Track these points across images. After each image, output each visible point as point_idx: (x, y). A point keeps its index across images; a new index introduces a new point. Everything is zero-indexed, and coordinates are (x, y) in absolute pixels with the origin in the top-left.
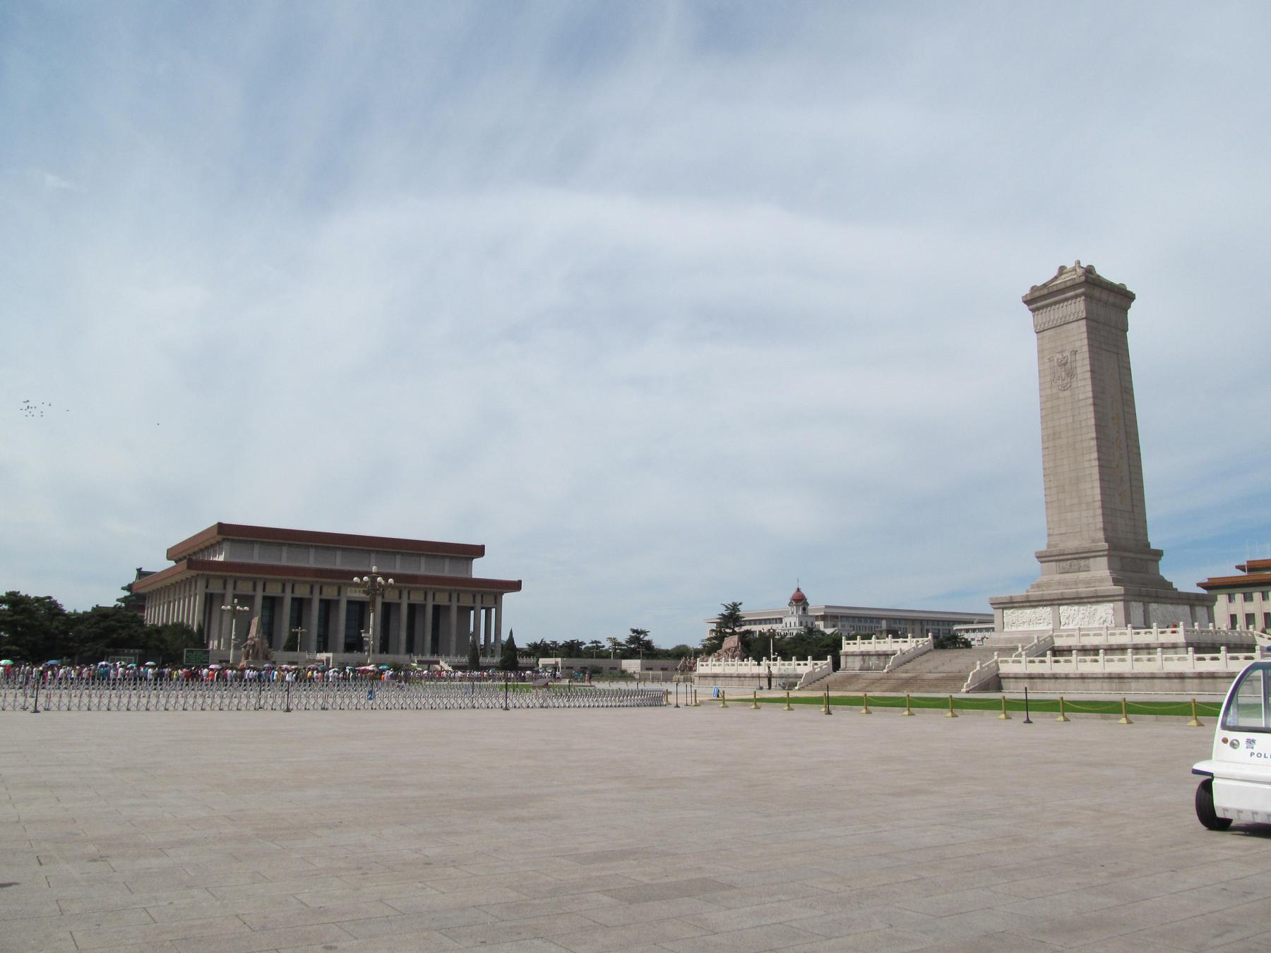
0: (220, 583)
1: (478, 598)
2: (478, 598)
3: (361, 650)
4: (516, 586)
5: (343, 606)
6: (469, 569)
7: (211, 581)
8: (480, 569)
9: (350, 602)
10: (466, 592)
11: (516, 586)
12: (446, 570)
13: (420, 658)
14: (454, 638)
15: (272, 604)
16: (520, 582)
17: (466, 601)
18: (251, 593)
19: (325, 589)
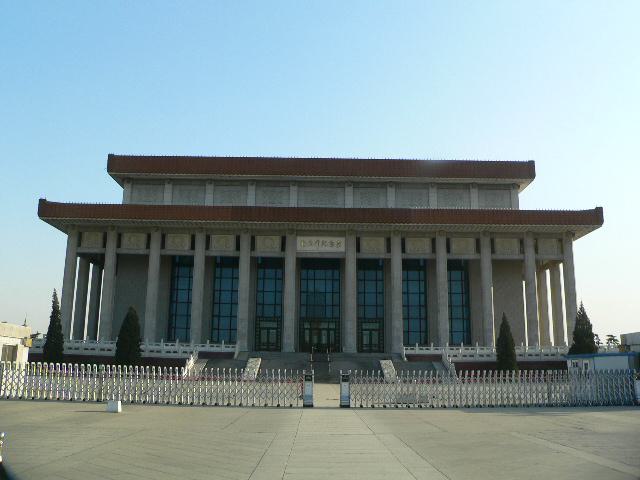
1: (529, 242)
2: (529, 242)
4: (592, 219)
5: (290, 267)
7: (86, 235)
8: (530, 199)
9: (306, 263)
10: (505, 235)
11: (592, 219)
12: (475, 202)
13: (417, 350)
15: (178, 266)
17: (508, 249)
18: (142, 252)
19: (259, 240)
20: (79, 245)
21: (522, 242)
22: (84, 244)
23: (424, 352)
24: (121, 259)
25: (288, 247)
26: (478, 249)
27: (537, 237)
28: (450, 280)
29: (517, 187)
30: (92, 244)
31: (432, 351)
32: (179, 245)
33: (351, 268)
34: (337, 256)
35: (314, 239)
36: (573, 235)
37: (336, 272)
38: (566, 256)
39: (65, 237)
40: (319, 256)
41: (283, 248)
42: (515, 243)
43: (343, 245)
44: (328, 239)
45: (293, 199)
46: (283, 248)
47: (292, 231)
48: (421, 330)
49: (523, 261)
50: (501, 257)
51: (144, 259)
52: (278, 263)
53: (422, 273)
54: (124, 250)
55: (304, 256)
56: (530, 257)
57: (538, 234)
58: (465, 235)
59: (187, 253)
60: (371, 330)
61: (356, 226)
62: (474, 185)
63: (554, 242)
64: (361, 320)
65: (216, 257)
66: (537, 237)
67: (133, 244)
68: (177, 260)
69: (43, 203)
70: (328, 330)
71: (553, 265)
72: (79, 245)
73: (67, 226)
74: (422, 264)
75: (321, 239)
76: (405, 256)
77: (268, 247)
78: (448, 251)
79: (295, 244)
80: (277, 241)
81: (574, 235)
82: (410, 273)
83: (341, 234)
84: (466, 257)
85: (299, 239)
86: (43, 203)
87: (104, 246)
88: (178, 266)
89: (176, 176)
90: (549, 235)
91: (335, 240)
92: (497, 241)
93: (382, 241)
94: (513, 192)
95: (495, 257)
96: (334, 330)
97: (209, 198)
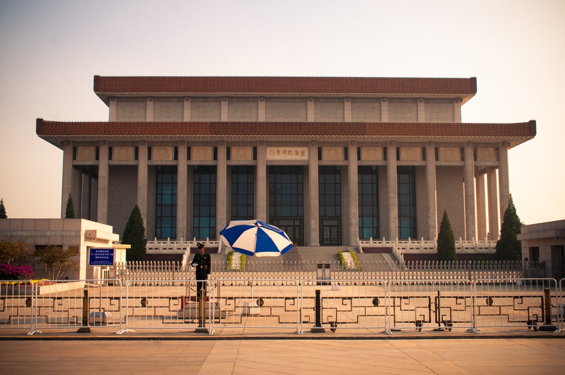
0: (92, 151)
1: (469, 152)
2: (469, 152)
3: (400, 238)
4: (527, 130)
6: (456, 113)
8: (471, 112)
9: (273, 170)
11: (527, 130)
12: (423, 115)
14: (394, 213)
15: (163, 175)
16: (532, 124)
17: (450, 157)
18: (132, 163)
20: (74, 158)
21: (462, 150)
22: (79, 156)
23: (378, 245)
24: (114, 170)
25: (259, 156)
26: (424, 157)
27: (476, 146)
28: (399, 183)
29: (460, 101)
30: (86, 157)
31: (384, 244)
32: (163, 157)
33: (314, 174)
34: (301, 164)
35: (281, 149)
36: (509, 145)
37: (300, 176)
38: (501, 163)
39: (62, 151)
41: (255, 157)
42: (457, 151)
43: (306, 154)
44: (293, 149)
45: (262, 114)
46: (255, 157)
47: (262, 142)
48: (374, 227)
49: (464, 167)
50: (443, 164)
51: (134, 169)
52: (251, 170)
53: (374, 176)
54: (114, 162)
55: (273, 164)
56: (470, 164)
57: (477, 143)
58: (412, 145)
59: (170, 163)
60: (330, 227)
61: (318, 137)
62: (420, 99)
63: (491, 150)
64: (322, 219)
65: (194, 166)
66: (476, 146)
67: (123, 156)
68: (160, 168)
69: (40, 122)
70: (294, 227)
71: (490, 170)
72: (74, 158)
73: (62, 142)
74: (374, 169)
75: (288, 149)
76: (361, 163)
77: (242, 156)
78: (398, 159)
79: (265, 153)
80: (249, 152)
81: (509, 144)
82: (364, 176)
84: (415, 164)
85: (269, 149)
86: (40, 122)
87: (97, 158)
88: (163, 175)
89: (157, 94)
90: (487, 145)
91: (300, 149)
92: (442, 150)
93: (340, 151)
94: (456, 105)
96: (300, 226)
97: (189, 114)
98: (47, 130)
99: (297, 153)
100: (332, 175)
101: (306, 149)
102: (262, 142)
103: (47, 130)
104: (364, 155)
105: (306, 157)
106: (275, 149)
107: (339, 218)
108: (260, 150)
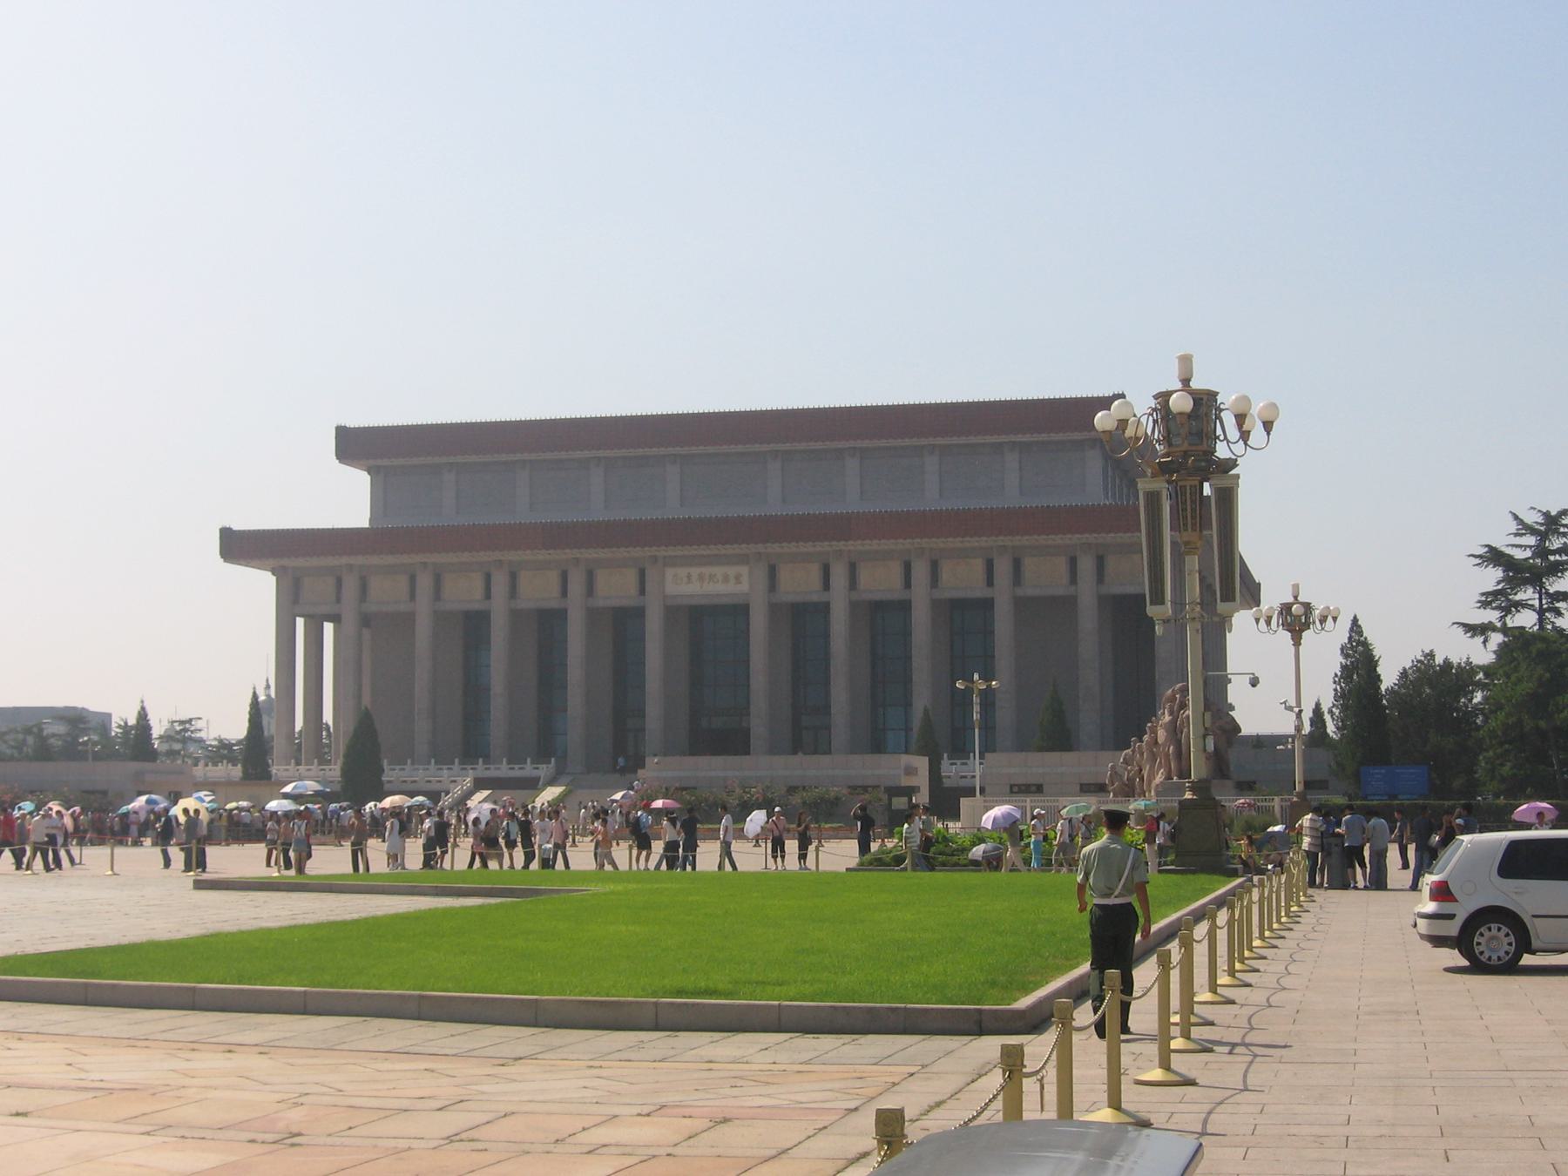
19: (602, 578)
20: (296, 601)
35: (695, 571)
40: (704, 602)
43: (745, 579)
44: (719, 571)
50: (1030, 592)
52: (639, 613)
75: (707, 570)
83: (743, 560)
85: (670, 572)
91: (732, 571)
95: (1020, 592)
98: (239, 546)
99: (726, 579)
100: (802, 623)
101: (744, 570)
102: (655, 559)
103: (239, 546)
104: (865, 576)
105: (744, 587)
106: (682, 572)
107: (1205, 665)
108: (651, 575)
